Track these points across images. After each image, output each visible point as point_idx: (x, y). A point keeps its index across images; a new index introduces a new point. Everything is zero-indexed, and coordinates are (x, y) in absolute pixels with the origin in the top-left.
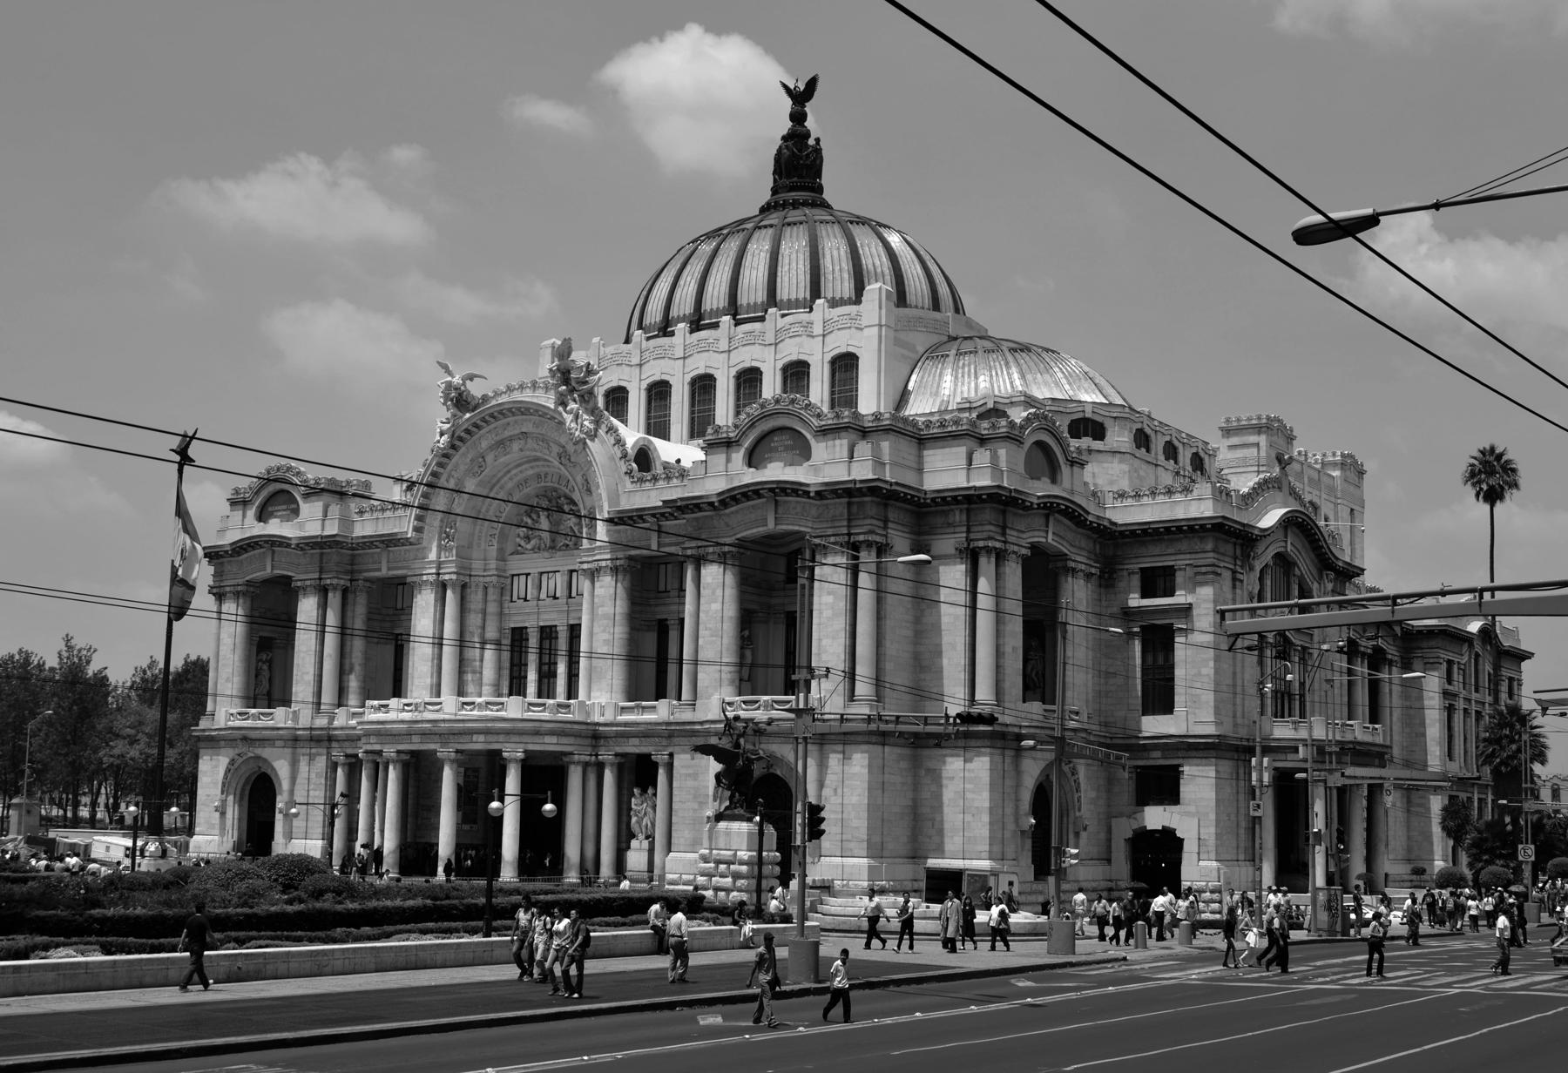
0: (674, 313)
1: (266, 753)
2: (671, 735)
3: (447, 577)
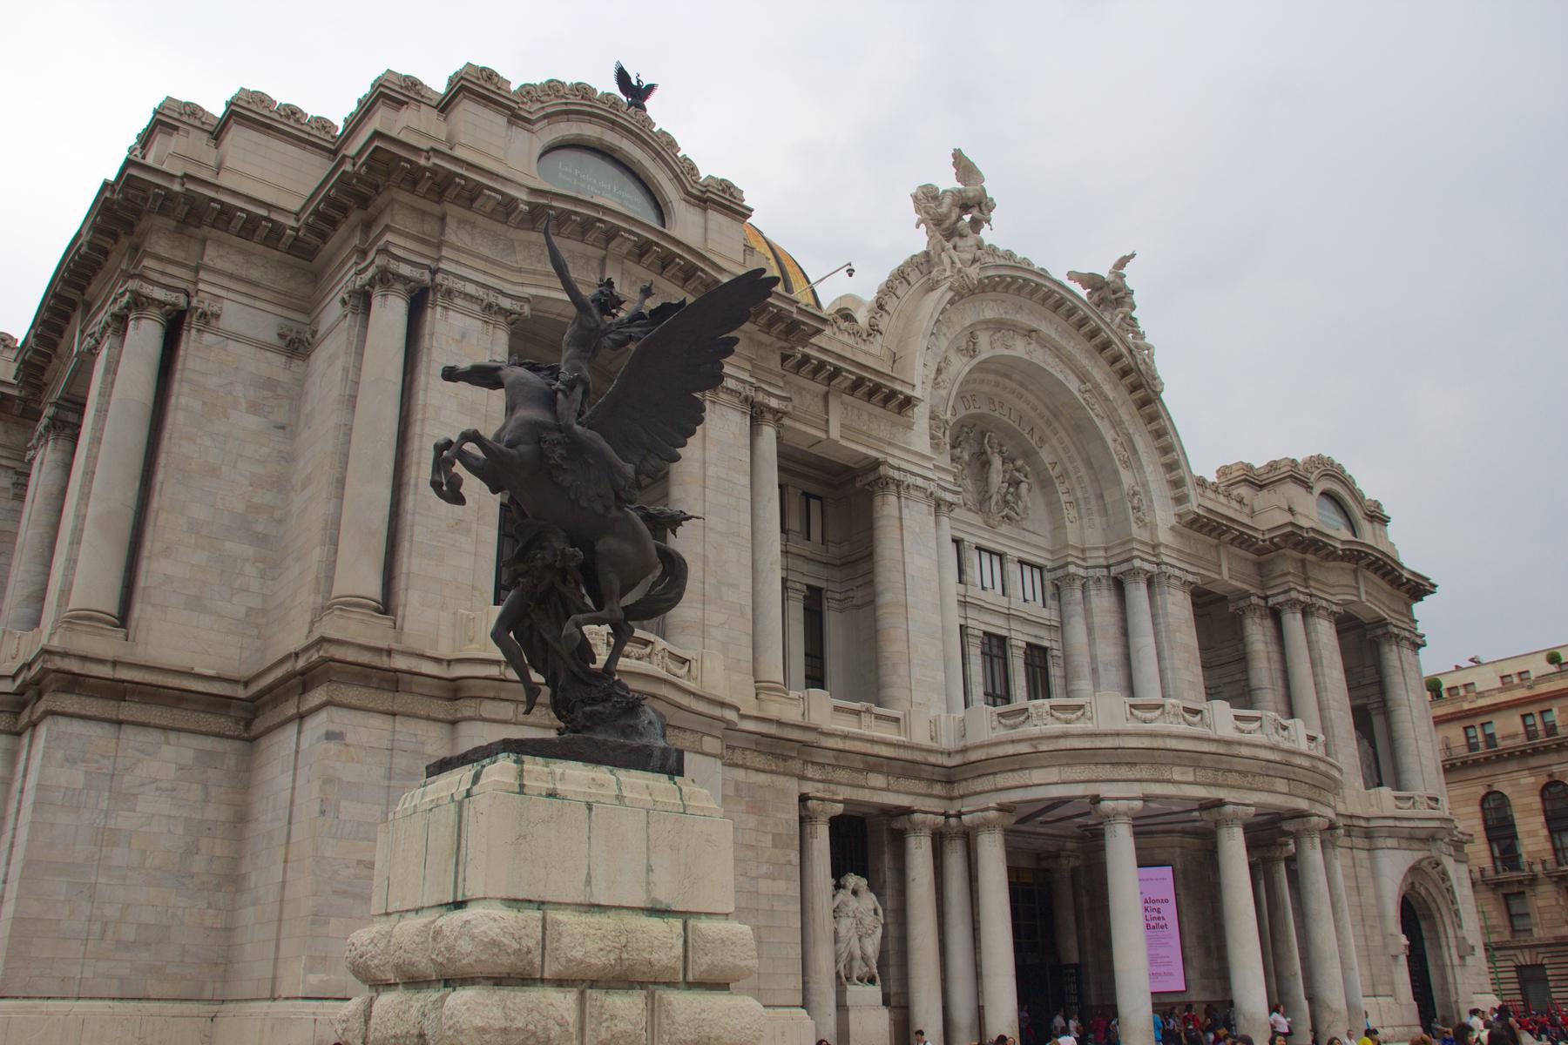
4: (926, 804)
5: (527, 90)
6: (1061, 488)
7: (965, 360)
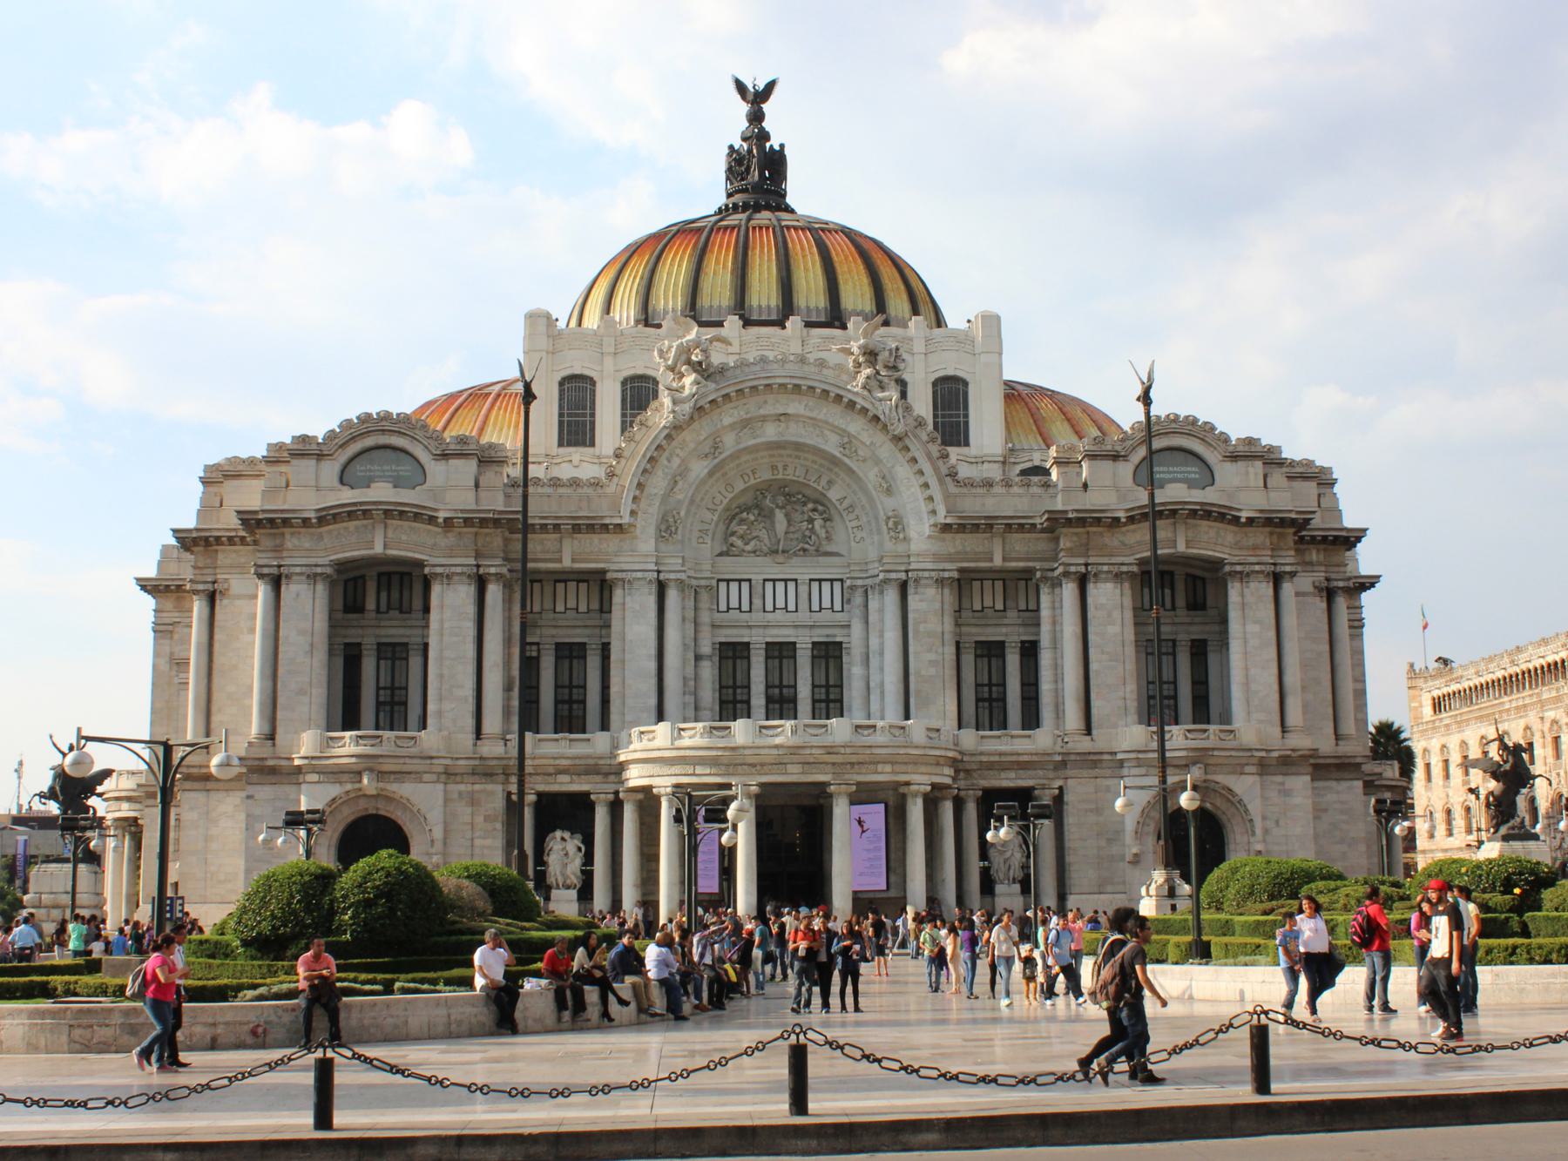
0: (705, 301)
1: (405, 790)
2: (1063, 764)
3: (672, 576)
4: (599, 790)
5: (331, 435)
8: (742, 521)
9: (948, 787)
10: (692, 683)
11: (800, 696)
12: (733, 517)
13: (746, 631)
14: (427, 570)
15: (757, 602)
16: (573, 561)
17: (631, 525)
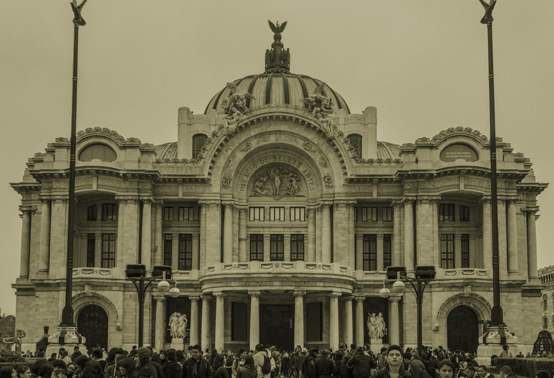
1: (105, 294)
3: (228, 202)
6: (307, 180)
7: (243, 153)
8: (261, 181)
9: (350, 295)
10: (237, 251)
11: (285, 257)
12: (257, 180)
13: (262, 230)
14: (116, 198)
15: (267, 217)
16: (183, 196)
17: (209, 180)
